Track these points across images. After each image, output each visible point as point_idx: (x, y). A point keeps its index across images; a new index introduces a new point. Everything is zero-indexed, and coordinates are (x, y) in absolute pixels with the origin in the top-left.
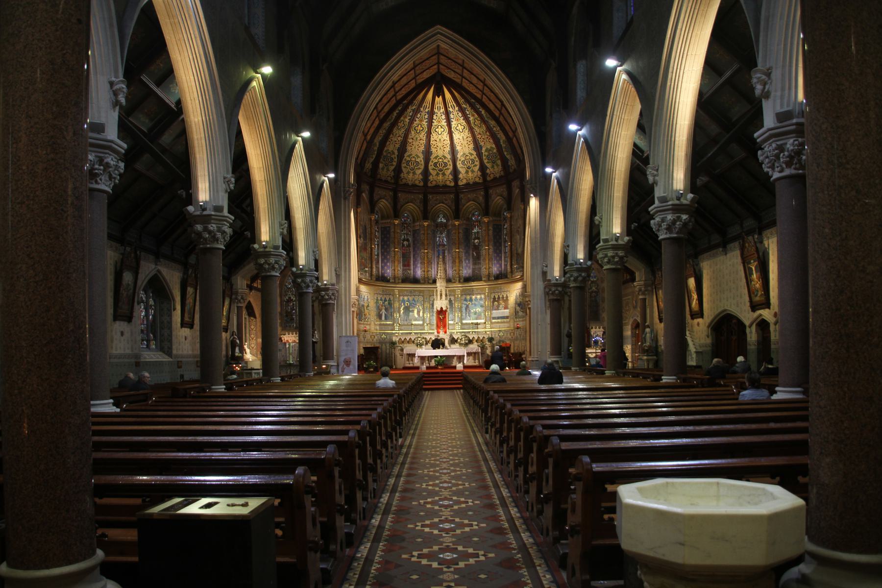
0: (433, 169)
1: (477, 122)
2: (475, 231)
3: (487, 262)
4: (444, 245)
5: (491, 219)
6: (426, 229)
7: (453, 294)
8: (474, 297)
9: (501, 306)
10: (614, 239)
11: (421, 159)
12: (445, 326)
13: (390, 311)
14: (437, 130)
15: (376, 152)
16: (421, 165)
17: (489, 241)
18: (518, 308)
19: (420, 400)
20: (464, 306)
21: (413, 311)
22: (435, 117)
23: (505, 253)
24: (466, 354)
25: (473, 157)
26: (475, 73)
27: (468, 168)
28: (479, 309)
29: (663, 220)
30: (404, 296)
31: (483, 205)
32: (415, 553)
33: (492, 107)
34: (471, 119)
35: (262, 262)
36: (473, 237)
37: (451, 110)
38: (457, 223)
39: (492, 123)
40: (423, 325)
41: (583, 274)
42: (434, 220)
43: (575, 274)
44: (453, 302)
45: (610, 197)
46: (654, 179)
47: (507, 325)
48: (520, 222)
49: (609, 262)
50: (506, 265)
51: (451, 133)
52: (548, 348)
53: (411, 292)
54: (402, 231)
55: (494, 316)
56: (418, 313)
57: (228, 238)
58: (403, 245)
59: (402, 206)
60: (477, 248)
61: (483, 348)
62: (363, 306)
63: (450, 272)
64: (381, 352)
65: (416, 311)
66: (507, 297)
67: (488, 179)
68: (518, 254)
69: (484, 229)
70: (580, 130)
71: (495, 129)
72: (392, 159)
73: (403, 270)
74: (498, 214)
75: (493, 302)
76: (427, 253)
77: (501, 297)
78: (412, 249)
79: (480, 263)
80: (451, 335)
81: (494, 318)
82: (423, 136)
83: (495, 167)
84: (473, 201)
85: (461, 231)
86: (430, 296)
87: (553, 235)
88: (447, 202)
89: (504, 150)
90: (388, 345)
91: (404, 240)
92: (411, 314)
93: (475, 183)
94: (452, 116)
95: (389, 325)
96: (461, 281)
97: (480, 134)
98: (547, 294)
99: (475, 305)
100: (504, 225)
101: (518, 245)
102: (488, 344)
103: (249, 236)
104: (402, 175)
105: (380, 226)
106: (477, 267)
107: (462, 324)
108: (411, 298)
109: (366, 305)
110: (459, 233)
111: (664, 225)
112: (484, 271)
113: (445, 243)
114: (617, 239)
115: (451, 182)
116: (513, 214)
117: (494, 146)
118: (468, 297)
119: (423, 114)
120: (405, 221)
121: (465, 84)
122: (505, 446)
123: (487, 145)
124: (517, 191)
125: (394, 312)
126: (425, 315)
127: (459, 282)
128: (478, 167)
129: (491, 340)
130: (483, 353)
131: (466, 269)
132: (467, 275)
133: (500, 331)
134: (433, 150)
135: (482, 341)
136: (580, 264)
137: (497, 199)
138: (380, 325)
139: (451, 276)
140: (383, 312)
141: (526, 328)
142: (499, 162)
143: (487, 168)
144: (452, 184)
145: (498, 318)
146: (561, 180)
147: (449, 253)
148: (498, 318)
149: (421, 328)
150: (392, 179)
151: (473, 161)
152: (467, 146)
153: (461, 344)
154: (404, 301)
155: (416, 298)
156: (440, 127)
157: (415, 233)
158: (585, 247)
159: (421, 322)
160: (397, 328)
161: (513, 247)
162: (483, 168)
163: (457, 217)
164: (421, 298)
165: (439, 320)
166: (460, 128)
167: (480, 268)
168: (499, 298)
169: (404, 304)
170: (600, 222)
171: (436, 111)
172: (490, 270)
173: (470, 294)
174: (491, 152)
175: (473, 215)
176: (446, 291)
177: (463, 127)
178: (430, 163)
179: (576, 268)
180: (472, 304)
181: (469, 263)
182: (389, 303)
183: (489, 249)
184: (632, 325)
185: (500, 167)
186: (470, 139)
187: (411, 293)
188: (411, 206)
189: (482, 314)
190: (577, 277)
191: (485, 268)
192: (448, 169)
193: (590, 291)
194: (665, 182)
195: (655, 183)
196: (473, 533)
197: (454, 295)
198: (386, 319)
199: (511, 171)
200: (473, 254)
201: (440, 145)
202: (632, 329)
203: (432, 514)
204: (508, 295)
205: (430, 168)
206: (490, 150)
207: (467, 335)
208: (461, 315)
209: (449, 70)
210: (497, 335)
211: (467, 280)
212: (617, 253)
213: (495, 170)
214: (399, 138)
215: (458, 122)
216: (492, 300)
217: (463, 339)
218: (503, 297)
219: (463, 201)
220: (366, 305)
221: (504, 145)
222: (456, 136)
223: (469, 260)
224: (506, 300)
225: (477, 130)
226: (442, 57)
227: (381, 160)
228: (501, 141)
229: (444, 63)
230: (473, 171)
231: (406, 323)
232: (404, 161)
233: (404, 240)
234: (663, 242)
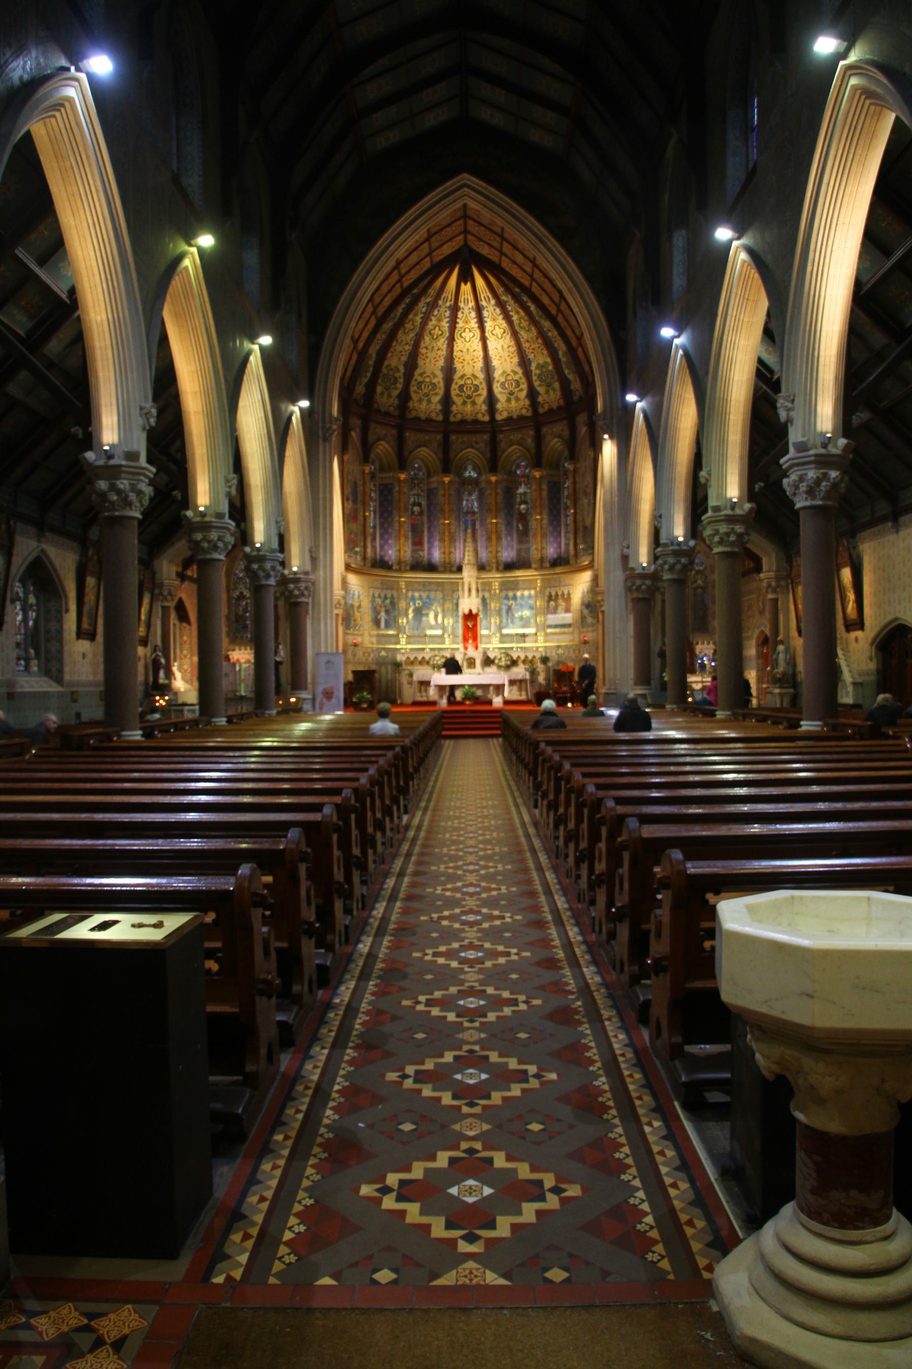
0: (458, 395)
1: (524, 324)
2: (521, 490)
3: (539, 539)
4: (474, 513)
5: (545, 473)
6: (447, 487)
7: (487, 588)
8: (519, 594)
9: (560, 608)
10: (729, 507)
11: (439, 380)
12: (475, 639)
14: (463, 335)
15: (371, 369)
17: (541, 506)
18: (586, 612)
20: (505, 608)
21: (427, 615)
22: (460, 315)
23: (567, 525)
24: (506, 683)
25: (516, 377)
26: (520, 247)
28: (527, 613)
29: (801, 479)
30: (413, 590)
31: (533, 451)
32: (422, 998)
33: (546, 300)
34: (515, 318)
36: (518, 500)
37: (484, 303)
38: (493, 479)
39: (546, 324)
40: (442, 636)
41: (683, 560)
42: (459, 474)
43: (671, 560)
44: (488, 601)
45: (723, 442)
46: (788, 415)
47: (568, 637)
48: (589, 479)
49: (721, 542)
50: (567, 545)
51: (484, 339)
52: (631, 674)
53: (424, 584)
54: (411, 490)
55: (550, 622)
58: (413, 513)
59: (411, 453)
60: (523, 518)
61: (533, 673)
62: (352, 606)
63: (484, 555)
64: (380, 680)
66: (569, 594)
67: (541, 411)
68: (585, 528)
69: (534, 488)
70: (678, 337)
71: (550, 334)
73: (413, 551)
74: (556, 465)
75: (549, 601)
76: (449, 524)
77: (560, 593)
78: (425, 518)
79: (528, 542)
80: (485, 653)
81: (550, 627)
82: (442, 343)
83: (551, 393)
84: (518, 444)
85: (499, 491)
86: (453, 591)
87: (638, 500)
88: (477, 446)
89: (564, 366)
90: (389, 668)
91: (414, 504)
92: (424, 619)
93: (521, 418)
94: (485, 313)
96: (501, 568)
97: (527, 341)
98: (629, 589)
99: (521, 606)
100: (565, 483)
101: (586, 513)
102: (540, 667)
104: (411, 404)
105: (377, 484)
106: (524, 546)
107: (502, 636)
108: (424, 595)
109: (356, 604)
110: (497, 494)
111: (803, 487)
112: (535, 554)
113: (476, 510)
114: (733, 506)
115: (484, 415)
116: (578, 465)
117: (549, 360)
118: (511, 594)
119: (442, 309)
120: (415, 475)
121: (506, 264)
122: (562, 828)
123: (540, 358)
124: (583, 430)
125: (399, 615)
127: (498, 570)
128: (524, 393)
129: (545, 660)
130: (533, 680)
131: (507, 550)
132: (509, 560)
133: (558, 647)
134: (457, 365)
135: (531, 662)
136: (679, 544)
137: (553, 442)
138: (378, 636)
139: (484, 560)
140: (383, 616)
141: (597, 643)
142: (557, 385)
143: (538, 394)
144: (487, 418)
145: (556, 626)
146: (649, 415)
147: (482, 524)
148: (556, 626)
149: (439, 640)
151: (518, 383)
152: (508, 359)
153: (499, 667)
154: (413, 599)
155: (432, 594)
156: (467, 330)
157: (431, 494)
158: (685, 519)
159: (439, 632)
160: (403, 641)
161: (578, 516)
162: (532, 394)
163: (493, 469)
164: (439, 595)
165: (466, 628)
166: (498, 331)
167: (529, 549)
168: (557, 595)
170: (707, 480)
171: (461, 305)
172: (544, 551)
173: (513, 589)
174: (544, 370)
175: (518, 466)
176: (477, 584)
177: (502, 331)
178: (454, 386)
179: (673, 550)
180: (517, 605)
181: (512, 540)
183: (542, 519)
184: (757, 639)
185: (558, 393)
186: (514, 349)
187: (425, 586)
188: (424, 452)
189: (532, 621)
190: (674, 565)
191: (536, 549)
192: (480, 395)
193: (694, 585)
194: (804, 420)
195: (789, 421)
196: (512, 967)
197: (489, 591)
198: (388, 626)
199: (575, 398)
200: (518, 527)
201: (468, 358)
202: (758, 646)
203: (449, 935)
204: (571, 591)
206: (543, 367)
207: (510, 652)
209: (481, 243)
210: (554, 654)
211: (509, 567)
212: (733, 529)
213: (550, 397)
214: (407, 347)
215: (496, 325)
216: (546, 598)
217: (503, 659)
218: (563, 595)
220: (356, 604)
221: (563, 360)
222: (492, 344)
223: (512, 537)
224: (568, 599)
225: (524, 335)
226: (470, 222)
227: (380, 381)
228: (560, 353)
229: (475, 232)
230: (517, 399)
231: (416, 633)
232: (413, 383)
233: (414, 504)
234: (801, 513)
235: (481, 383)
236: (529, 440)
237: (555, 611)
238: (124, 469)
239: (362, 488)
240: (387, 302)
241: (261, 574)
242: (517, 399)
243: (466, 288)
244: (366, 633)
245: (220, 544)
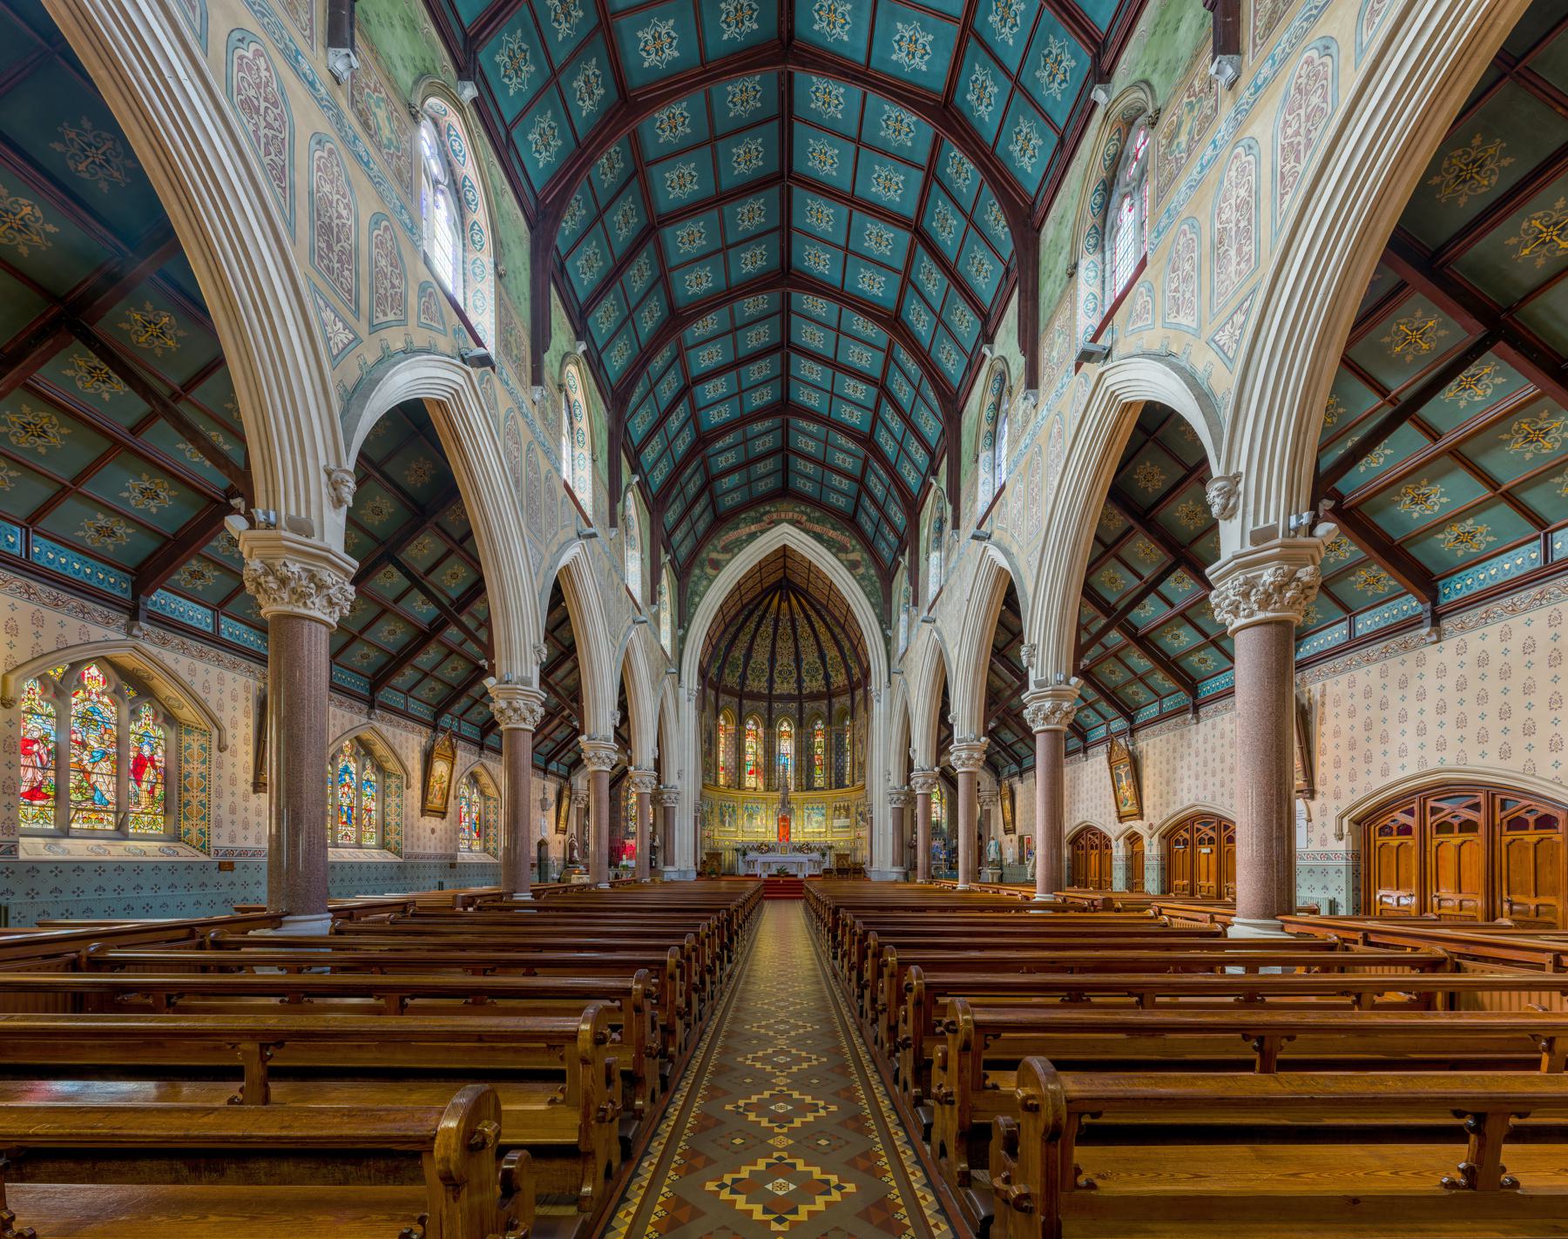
19: (760, 911)
32: (750, 1056)
57: (538, 720)
122: (846, 960)
142: (843, 671)
164: (764, 806)
240: (733, 612)
243: (784, 605)
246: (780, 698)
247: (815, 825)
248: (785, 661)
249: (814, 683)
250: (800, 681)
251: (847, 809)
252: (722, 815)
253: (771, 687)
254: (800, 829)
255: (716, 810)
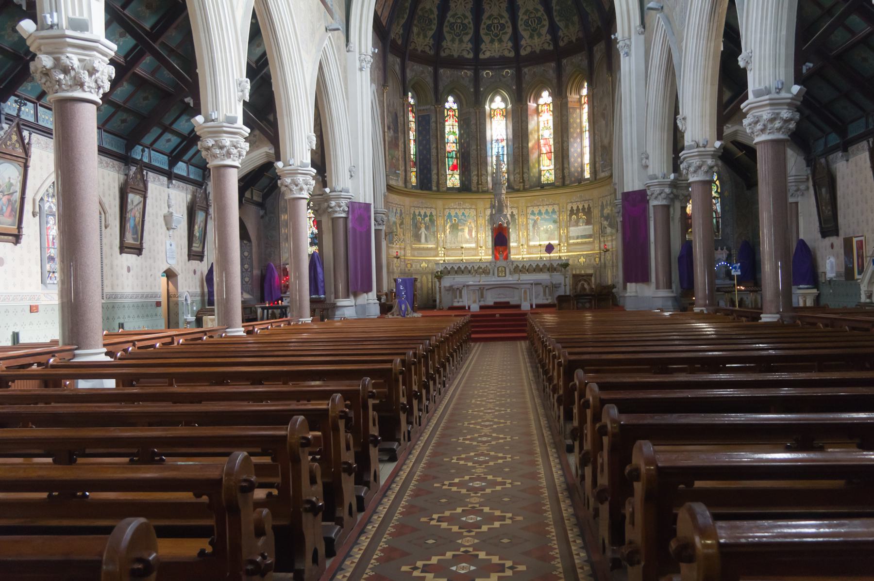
0: (486, 34)
13: (432, 230)
15: (408, 11)
16: (470, 28)
20: (531, 222)
21: (462, 230)
27: (532, 30)
35: (210, 145)
44: (516, 217)
56: (470, 232)
64: (422, 287)
65: (466, 230)
72: (430, 21)
90: (430, 277)
92: (460, 233)
93: (543, 51)
95: (431, 249)
103: (192, 105)
104: (444, 44)
107: (528, 246)
125: (437, 231)
126: (479, 236)
142: (576, 19)
144: (512, 54)
149: (473, 252)
150: (431, 48)
154: (450, 216)
155: (467, 212)
159: (473, 245)
160: (441, 252)
164: (473, 213)
169: (451, 221)
178: (482, 26)
182: (431, 220)
205: (482, 32)
208: (528, 235)
219: (526, 76)
227: (415, 22)
231: (453, 246)
232: (446, 24)
235: (507, 22)
236: (551, 72)
237: (577, 224)
238: (68, 40)
239: (402, 118)
241: (294, 188)
242: (539, 35)
244: (408, 248)
245: (234, 151)
246: (491, 63)
247: (543, 235)
248: (495, 11)
249: (536, 40)
250: (516, 38)
251: (588, 212)
252: (417, 227)
253: (477, 50)
254: (523, 241)
255: (408, 221)
